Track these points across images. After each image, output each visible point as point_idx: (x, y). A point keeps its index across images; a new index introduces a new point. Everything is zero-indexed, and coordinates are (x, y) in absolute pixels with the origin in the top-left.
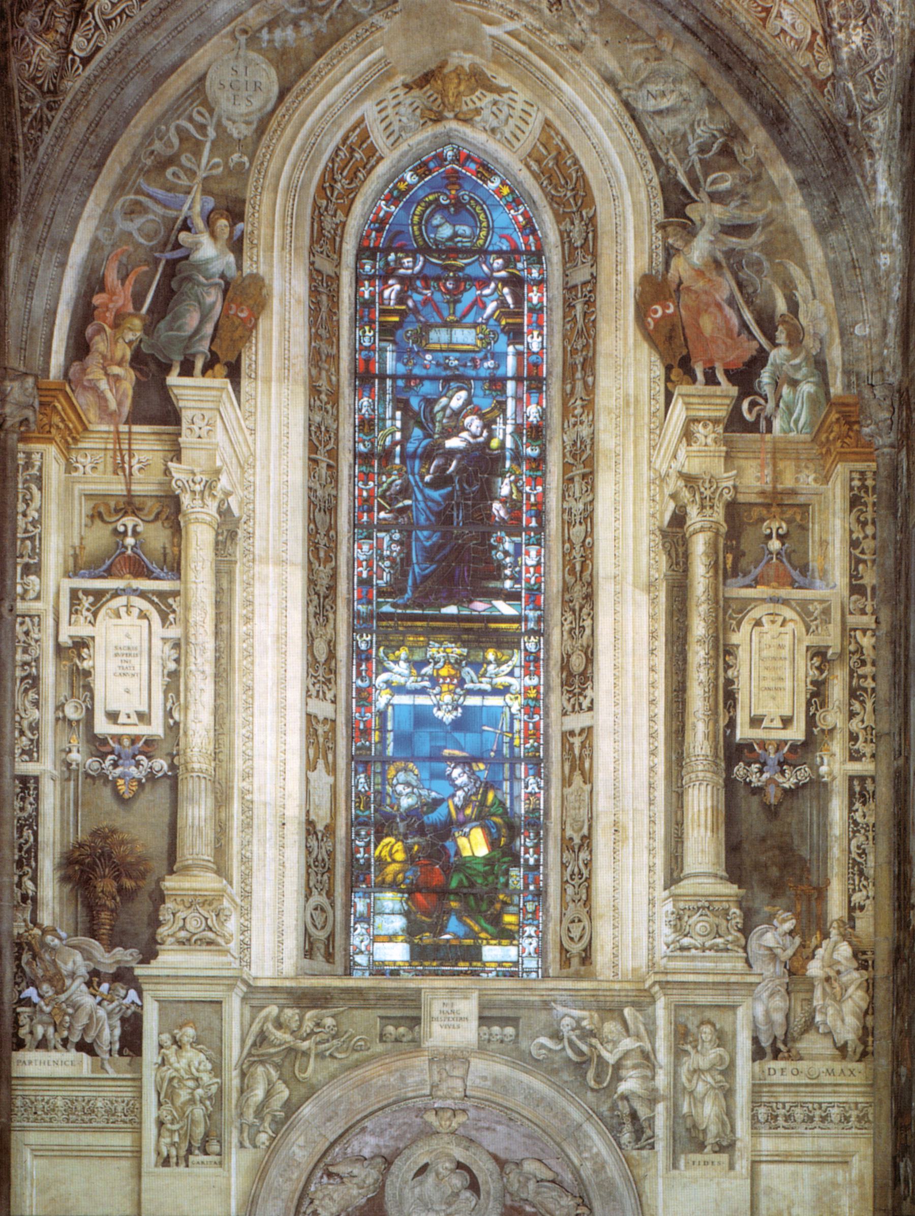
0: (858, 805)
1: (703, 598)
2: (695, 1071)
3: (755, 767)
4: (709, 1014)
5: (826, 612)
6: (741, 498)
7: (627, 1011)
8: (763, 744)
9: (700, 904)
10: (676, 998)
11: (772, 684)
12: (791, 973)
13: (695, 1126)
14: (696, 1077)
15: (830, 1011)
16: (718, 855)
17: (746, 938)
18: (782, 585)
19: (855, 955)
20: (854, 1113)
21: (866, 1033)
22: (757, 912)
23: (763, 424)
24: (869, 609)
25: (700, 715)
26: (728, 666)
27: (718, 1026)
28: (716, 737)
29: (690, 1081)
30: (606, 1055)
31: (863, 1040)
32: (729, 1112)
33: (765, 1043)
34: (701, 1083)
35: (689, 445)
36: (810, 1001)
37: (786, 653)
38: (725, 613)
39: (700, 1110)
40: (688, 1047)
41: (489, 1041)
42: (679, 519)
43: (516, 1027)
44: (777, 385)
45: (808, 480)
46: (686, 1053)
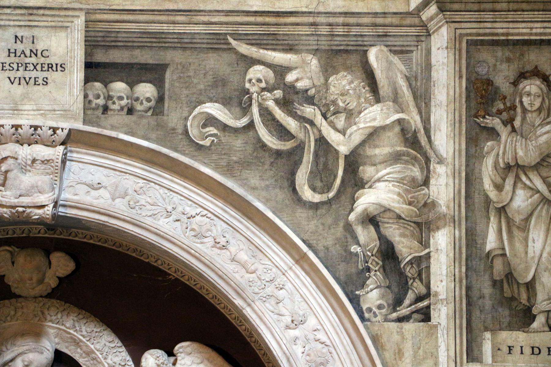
2: (508, 167)
7: (373, 55)
10: (470, 28)
13: (510, 276)
14: (510, 181)
29: (499, 188)
30: (333, 137)
34: (521, 193)
39: (519, 246)
40: (495, 122)
41: (106, 109)
43: (159, 83)
46: (493, 133)
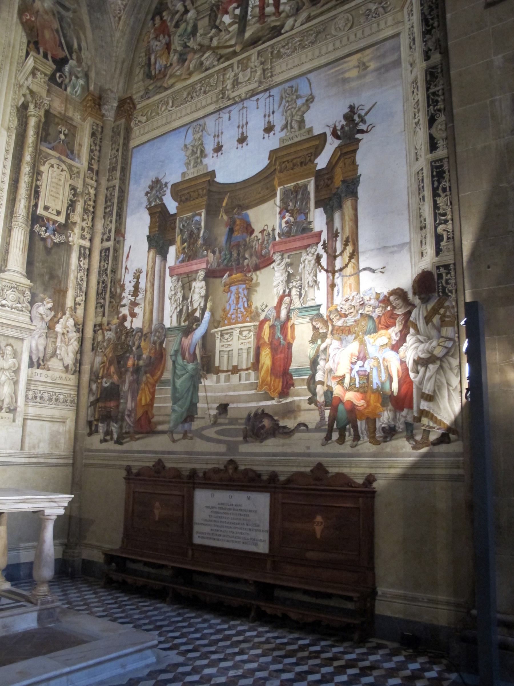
0: (82, 259)
1: (31, 145)
3: (44, 228)
4: (11, 341)
5: (78, 173)
6: (51, 111)
8: (48, 219)
9: (13, 285)
11: (54, 195)
12: (49, 328)
15: (63, 349)
16: (23, 264)
17: (32, 307)
18: (63, 155)
19: (75, 325)
20: (69, 399)
21: (79, 362)
22: (37, 296)
23: (63, 86)
24: (94, 178)
25: (23, 196)
26: (37, 180)
27: (14, 348)
28: (29, 208)
31: (75, 364)
32: (15, 392)
33: (35, 360)
35: (33, 77)
36: (55, 342)
37: (61, 183)
38: (39, 156)
42: (25, 107)
44: (71, 74)
45: (77, 117)
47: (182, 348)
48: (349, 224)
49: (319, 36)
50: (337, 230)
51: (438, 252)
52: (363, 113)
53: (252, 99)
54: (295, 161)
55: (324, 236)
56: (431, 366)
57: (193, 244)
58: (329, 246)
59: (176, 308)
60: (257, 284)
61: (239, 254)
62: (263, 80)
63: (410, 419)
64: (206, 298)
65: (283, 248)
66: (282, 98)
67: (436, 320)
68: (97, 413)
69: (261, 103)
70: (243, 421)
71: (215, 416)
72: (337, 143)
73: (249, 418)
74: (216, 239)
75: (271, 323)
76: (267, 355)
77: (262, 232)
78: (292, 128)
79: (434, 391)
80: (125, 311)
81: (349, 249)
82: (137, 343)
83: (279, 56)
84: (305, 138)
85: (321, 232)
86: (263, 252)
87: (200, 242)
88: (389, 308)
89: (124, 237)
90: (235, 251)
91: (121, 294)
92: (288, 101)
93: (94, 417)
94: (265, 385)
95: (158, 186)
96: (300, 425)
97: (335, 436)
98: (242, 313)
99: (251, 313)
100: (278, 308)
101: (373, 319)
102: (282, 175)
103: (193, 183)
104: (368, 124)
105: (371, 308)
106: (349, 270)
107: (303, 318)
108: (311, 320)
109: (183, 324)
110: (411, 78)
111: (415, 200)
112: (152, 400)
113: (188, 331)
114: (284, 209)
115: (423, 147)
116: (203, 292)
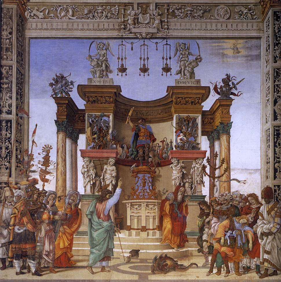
47: (97, 210)
48: (224, 151)
49: (206, 14)
50: (217, 152)
51: (275, 177)
52: (235, 83)
53: (151, 40)
54: (187, 99)
55: (208, 154)
56: (270, 237)
57: (103, 138)
58: (212, 162)
59: (89, 181)
60: (160, 176)
61: (144, 153)
62: (160, 29)
63: (258, 263)
64: (117, 178)
65: (177, 155)
66: (177, 50)
67: (273, 213)
68: (10, 252)
69: (160, 46)
70: (151, 261)
71: (129, 258)
72: (217, 97)
73: (156, 259)
74: (124, 138)
75: (171, 202)
76: (168, 221)
77: (163, 142)
78: (185, 75)
79: (271, 249)
80: (36, 176)
81: (225, 166)
82: (50, 202)
83: (174, 15)
84: (195, 85)
85: (206, 151)
86: (164, 155)
87: (109, 137)
88: (247, 204)
89: (28, 115)
90: (141, 150)
91: (29, 162)
92: (182, 54)
93: (7, 255)
94: (167, 240)
95: (64, 82)
96: (192, 264)
97: (215, 271)
98: (148, 193)
99: (155, 194)
100: (176, 193)
101: (238, 208)
102: (177, 106)
103: (100, 90)
104: (238, 91)
105: (237, 202)
106: (224, 178)
107: (193, 202)
108: (199, 204)
109: (97, 194)
110: (266, 70)
111: (264, 146)
112: (71, 244)
113: (102, 199)
114: (179, 130)
115: (270, 115)
116: (114, 174)
